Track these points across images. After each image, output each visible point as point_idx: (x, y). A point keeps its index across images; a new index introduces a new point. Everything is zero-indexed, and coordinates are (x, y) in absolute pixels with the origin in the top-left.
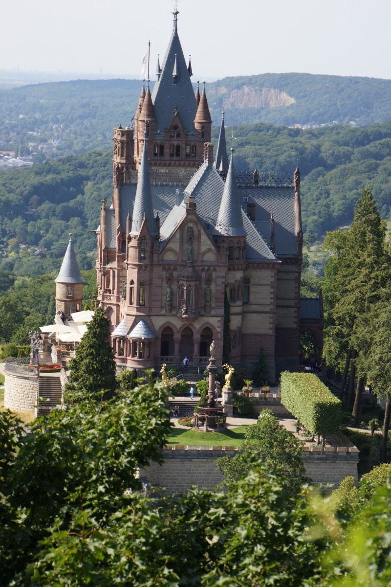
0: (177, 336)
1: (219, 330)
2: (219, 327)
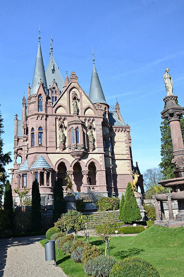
1: (101, 163)
2: (101, 161)
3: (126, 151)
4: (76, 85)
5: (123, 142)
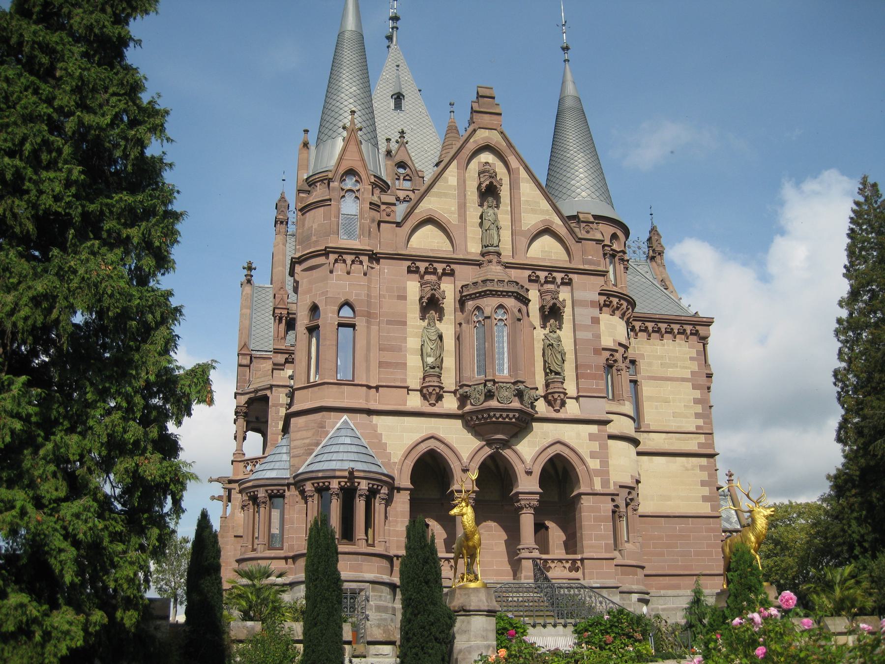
0: (465, 481)
2: (593, 455)
3: (693, 419)
4: (494, 138)
5: (684, 380)
